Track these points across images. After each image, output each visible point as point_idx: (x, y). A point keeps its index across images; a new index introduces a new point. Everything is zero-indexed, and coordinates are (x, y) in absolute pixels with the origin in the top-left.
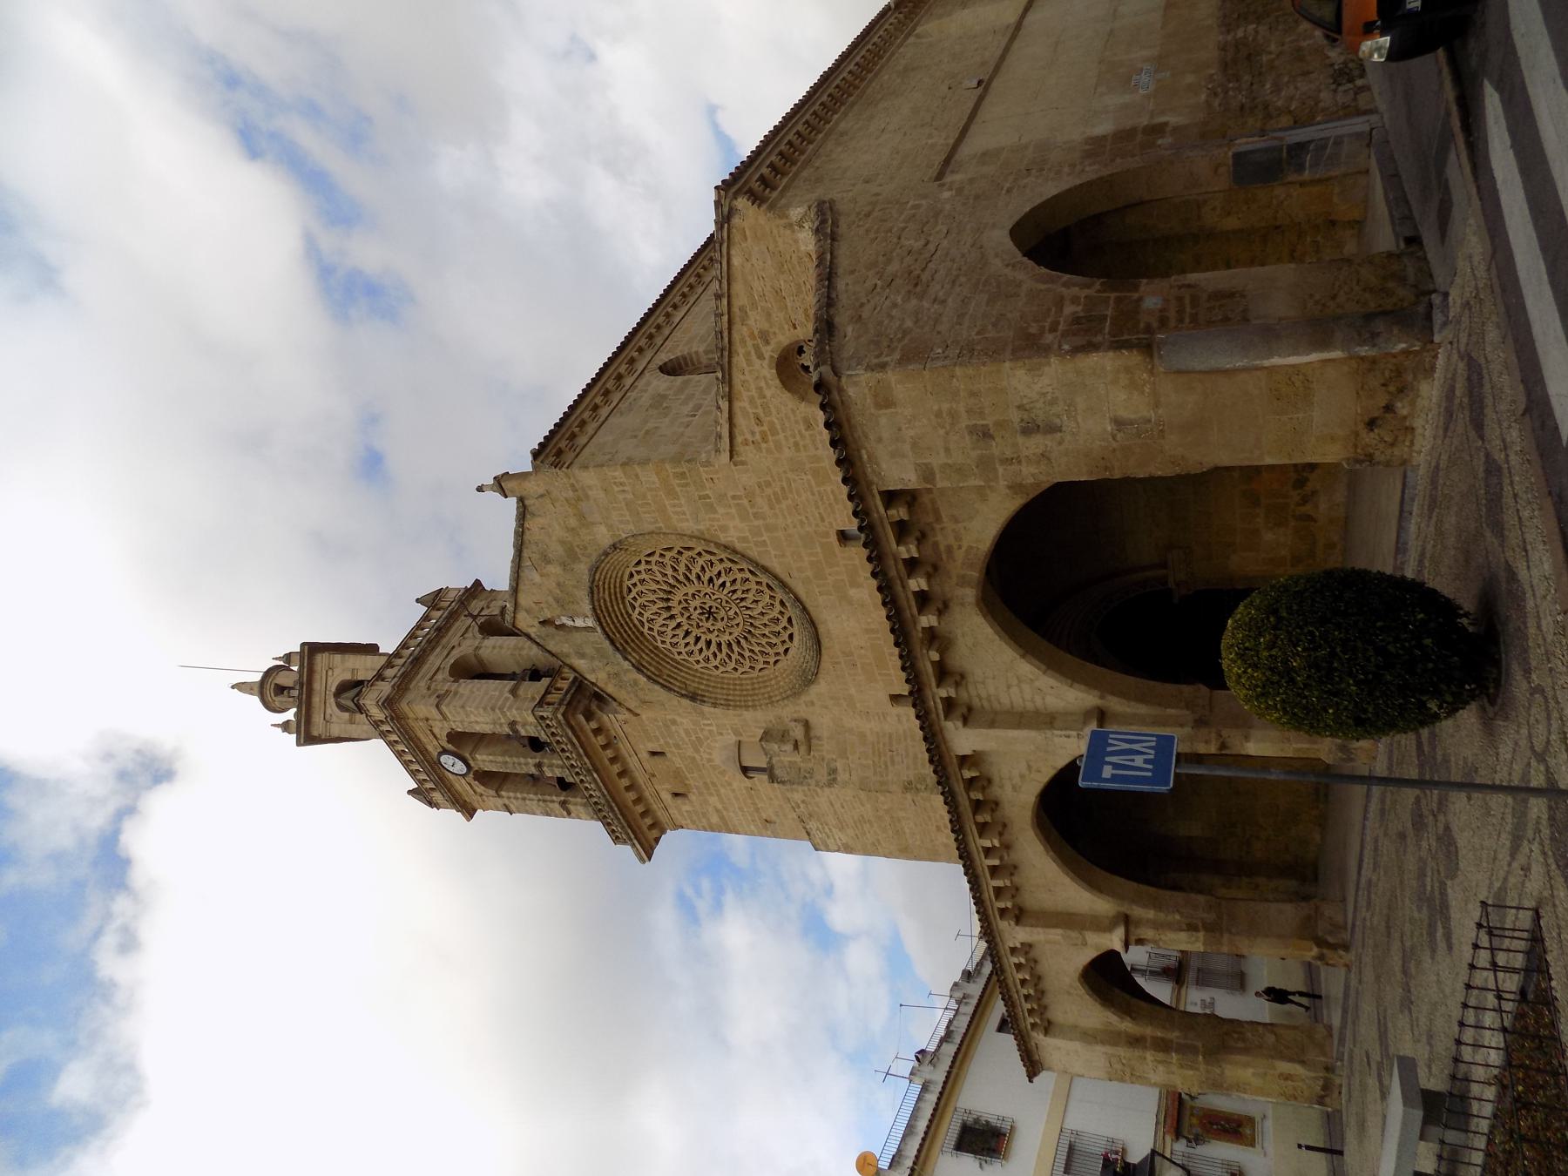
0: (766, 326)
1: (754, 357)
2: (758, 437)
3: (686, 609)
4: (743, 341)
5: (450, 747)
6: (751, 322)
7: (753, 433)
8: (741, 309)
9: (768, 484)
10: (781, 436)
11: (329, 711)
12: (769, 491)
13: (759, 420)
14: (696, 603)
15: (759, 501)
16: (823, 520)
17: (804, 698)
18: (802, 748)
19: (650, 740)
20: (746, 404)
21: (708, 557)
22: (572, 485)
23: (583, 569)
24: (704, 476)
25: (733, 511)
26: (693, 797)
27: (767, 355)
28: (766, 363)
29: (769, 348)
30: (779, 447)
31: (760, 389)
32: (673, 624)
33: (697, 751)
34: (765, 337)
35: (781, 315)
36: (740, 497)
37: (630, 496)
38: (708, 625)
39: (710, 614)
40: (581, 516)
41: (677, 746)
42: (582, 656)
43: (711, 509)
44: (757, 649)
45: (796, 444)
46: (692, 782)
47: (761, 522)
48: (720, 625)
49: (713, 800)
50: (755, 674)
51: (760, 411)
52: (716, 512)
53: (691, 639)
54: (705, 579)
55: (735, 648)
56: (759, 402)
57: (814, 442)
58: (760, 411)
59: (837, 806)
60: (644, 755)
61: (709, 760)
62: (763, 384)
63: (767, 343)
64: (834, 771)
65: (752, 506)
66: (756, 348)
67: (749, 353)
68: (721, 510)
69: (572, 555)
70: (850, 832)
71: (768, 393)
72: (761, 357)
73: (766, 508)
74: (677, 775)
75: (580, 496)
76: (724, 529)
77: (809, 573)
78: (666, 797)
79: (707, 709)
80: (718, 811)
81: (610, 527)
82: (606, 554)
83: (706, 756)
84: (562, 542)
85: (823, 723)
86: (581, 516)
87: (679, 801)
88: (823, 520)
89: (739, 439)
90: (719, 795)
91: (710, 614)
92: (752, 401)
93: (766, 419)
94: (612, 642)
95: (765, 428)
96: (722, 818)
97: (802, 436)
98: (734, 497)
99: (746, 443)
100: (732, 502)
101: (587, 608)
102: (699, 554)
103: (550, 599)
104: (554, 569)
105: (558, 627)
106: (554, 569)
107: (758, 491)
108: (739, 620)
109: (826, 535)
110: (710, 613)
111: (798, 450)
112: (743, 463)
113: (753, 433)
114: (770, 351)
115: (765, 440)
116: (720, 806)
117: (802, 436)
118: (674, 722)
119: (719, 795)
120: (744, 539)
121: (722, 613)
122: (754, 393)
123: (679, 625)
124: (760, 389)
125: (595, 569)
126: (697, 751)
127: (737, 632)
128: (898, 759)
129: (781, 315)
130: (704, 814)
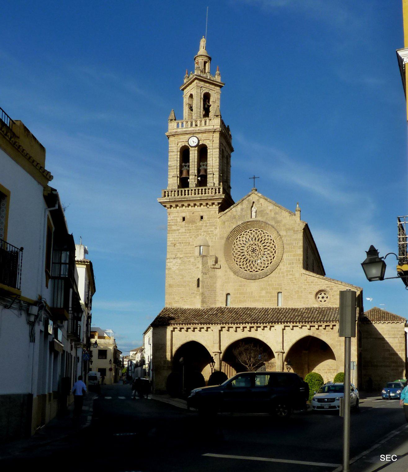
0: (334, 290)
1: (327, 286)
2: (308, 281)
4: (331, 285)
5: (200, 143)
6: (335, 287)
7: (309, 280)
8: (338, 286)
9: (296, 280)
10: (308, 286)
11: (204, 89)
12: (294, 279)
13: (312, 282)
14: (257, 248)
15: (291, 277)
16: (285, 289)
17: (228, 270)
18: (213, 266)
19: (208, 218)
20: (316, 281)
21: (273, 257)
22: (298, 231)
23: (272, 223)
24: (299, 265)
25: (289, 269)
26: (184, 223)
27: (327, 288)
28: (326, 288)
29: (329, 289)
30: (305, 285)
31: (320, 285)
33: (204, 232)
34: (331, 289)
35: (336, 294)
36: (292, 272)
37: (294, 244)
38: (250, 249)
39: (254, 250)
40: (289, 229)
41: (206, 226)
42: (242, 209)
43: (290, 264)
44: (242, 260)
45: (306, 289)
46: (190, 225)
47: (285, 274)
48: (250, 253)
49: (183, 230)
50: (233, 257)
51: (314, 283)
52: (289, 265)
53: (245, 242)
56: (317, 284)
57: (306, 293)
58: (314, 283)
59: (189, 271)
60: (202, 214)
61: (201, 235)
62: (321, 286)
63: (330, 289)
64: (206, 274)
65: (290, 274)
66: (329, 287)
67: (328, 285)
68: (289, 266)
69: (277, 222)
70: (177, 272)
71: (318, 286)
72: (327, 287)
73: (289, 277)
74: (193, 222)
75: (295, 232)
76: (284, 265)
77: (270, 283)
78: (184, 215)
79: (223, 241)
80: (178, 230)
81: (286, 236)
82: (278, 232)
83: (202, 234)
84: (281, 220)
85: (219, 272)
86: (289, 229)
87: (182, 218)
88: (285, 289)
89: (308, 276)
90: (186, 232)
91: (254, 250)
92: (316, 282)
93: (312, 284)
94: (248, 222)
95: (310, 283)
96: (175, 230)
97: (307, 291)
98: (292, 271)
99: (307, 278)
100: (291, 270)
101: (259, 218)
102: (273, 255)
103: (262, 209)
104: (273, 215)
106: (273, 215)
107: (294, 277)
108: (252, 258)
109: (281, 289)
111: (304, 289)
112: (302, 276)
113: (309, 280)
114: (328, 289)
115: (307, 282)
116: (180, 231)
117: (307, 291)
118: (216, 228)
119: (186, 232)
120: (280, 269)
121: (254, 254)
122: (319, 283)
124: (320, 285)
125: (273, 227)
126: (204, 232)
127: (248, 257)
128: (210, 292)
129: (336, 294)
130: (177, 225)
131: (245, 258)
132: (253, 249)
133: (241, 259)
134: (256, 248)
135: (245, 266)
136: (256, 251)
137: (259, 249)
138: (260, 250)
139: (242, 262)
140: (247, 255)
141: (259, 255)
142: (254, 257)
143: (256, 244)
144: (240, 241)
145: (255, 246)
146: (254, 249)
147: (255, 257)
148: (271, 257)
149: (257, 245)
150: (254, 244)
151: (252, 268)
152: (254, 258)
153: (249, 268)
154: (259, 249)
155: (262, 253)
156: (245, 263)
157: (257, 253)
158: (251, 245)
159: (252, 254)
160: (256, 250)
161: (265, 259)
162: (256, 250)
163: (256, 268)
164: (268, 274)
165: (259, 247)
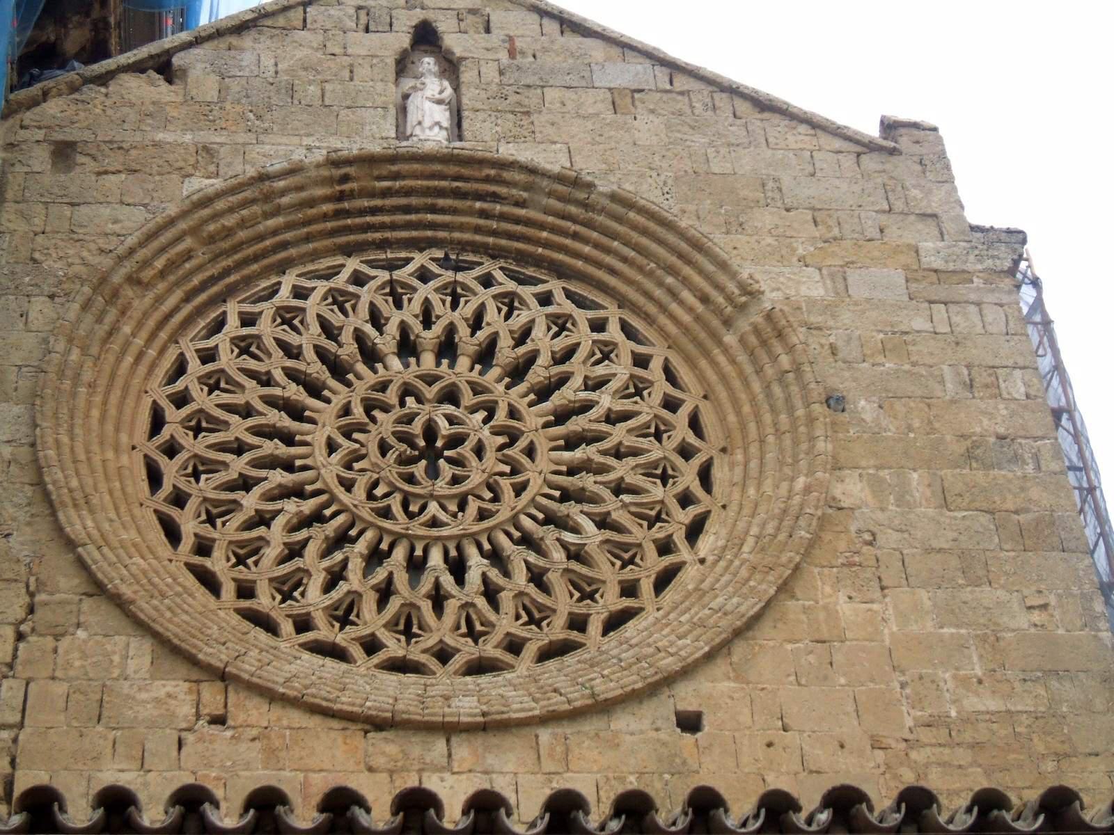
3: (450, 396)
32: (386, 342)
54: (587, 481)
55: (278, 477)
105: (403, 66)
110: (431, 454)
123: (371, 356)
131: (317, 517)
132: (417, 427)
133: (262, 520)
134: (451, 420)
135: (314, 598)
136: (466, 450)
137: (501, 440)
138: (515, 452)
139: (271, 553)
140: (348, 486)
141: (496, 499)
142: (433, 508)
143: (450, 396)
144: (244, 346)
145: (449, 409)
146: (430, 432)
147: (443, 516)
148: (658, 518)
149: (468, 398)
150: (430, 392)
151: (407, 627)
152: (434, 523)
153: (371, 620)
154: (501, 440)
155: (537, 474)
156: (314, 563)
157: (476, 478)
158: (391, 396)
159: (411, 479)
160: (456, 441)
161: (592, 536)
162: (456, 441)
163: (473, 635)
164: (669, 663)
165: (501, 417)
